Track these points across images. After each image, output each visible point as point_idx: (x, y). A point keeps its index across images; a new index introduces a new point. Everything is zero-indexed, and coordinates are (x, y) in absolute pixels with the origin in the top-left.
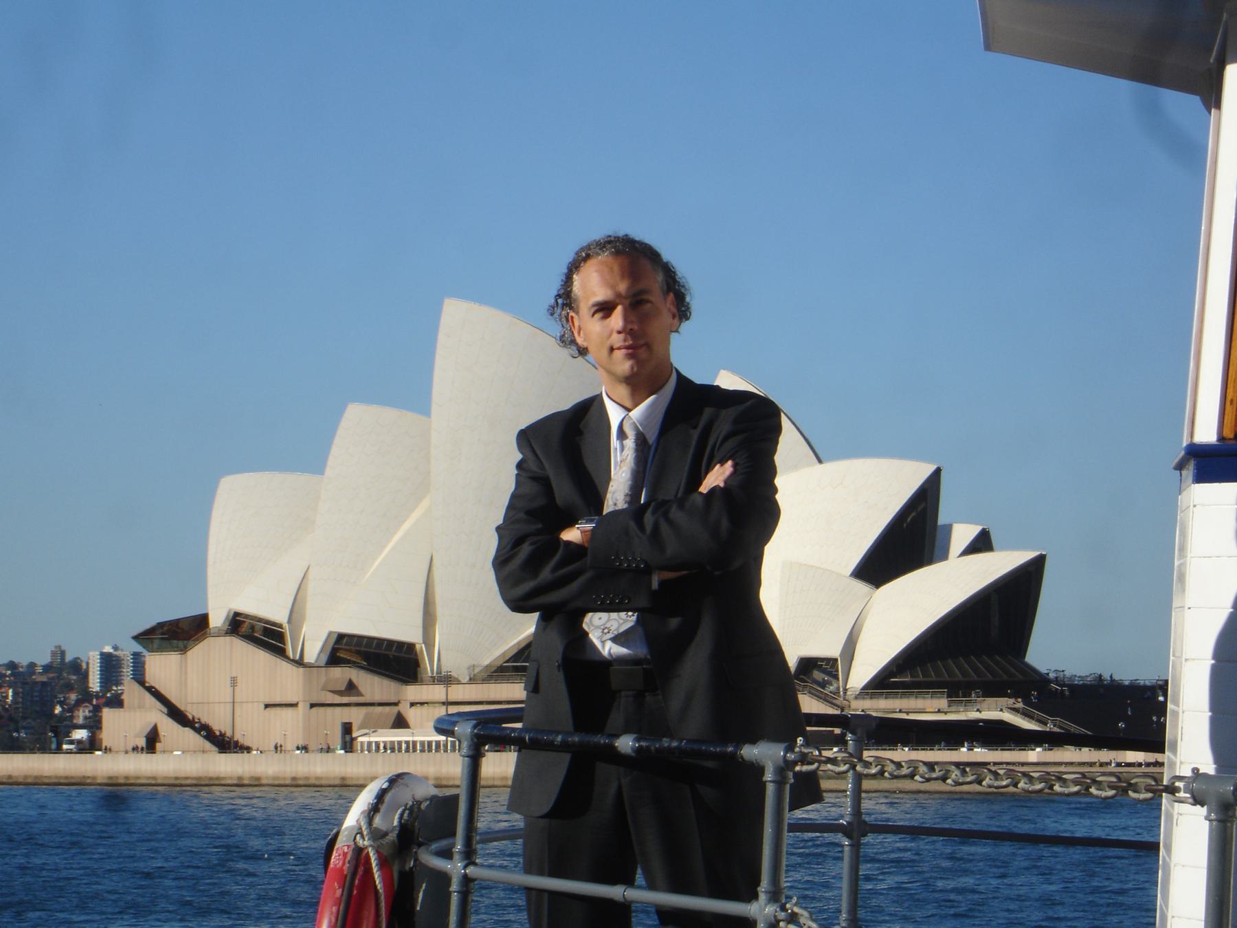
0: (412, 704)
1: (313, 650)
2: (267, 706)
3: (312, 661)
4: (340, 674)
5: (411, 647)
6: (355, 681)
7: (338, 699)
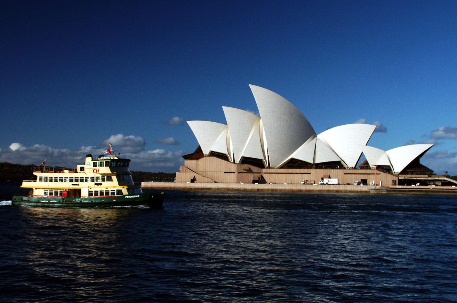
0: (264, 173)
1: (238, 160)
2: (224, 173)
3: (238, 163)
4: (246, 166)
5: (261, 160)
6: (250, 167)
7: (246, 172)
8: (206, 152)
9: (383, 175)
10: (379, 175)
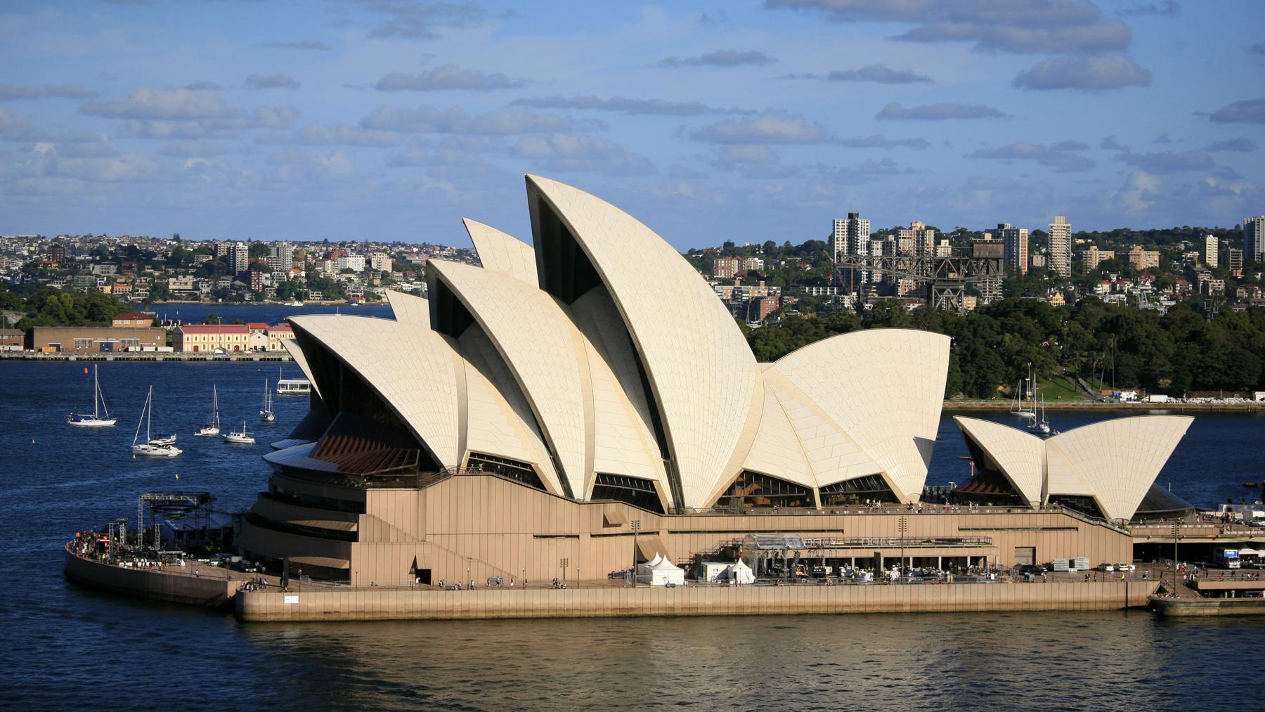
1: (581, 487)
5: (648, 483)
8: (447, 455)
9: (1086, 529)
10: (1074, 532)
